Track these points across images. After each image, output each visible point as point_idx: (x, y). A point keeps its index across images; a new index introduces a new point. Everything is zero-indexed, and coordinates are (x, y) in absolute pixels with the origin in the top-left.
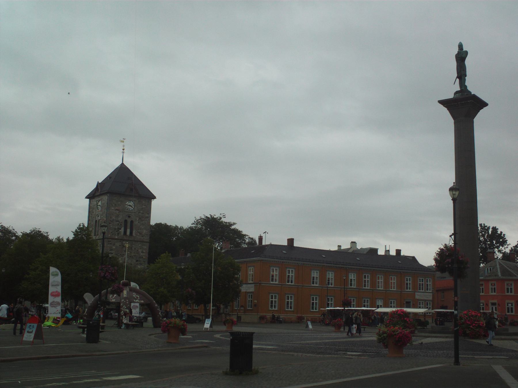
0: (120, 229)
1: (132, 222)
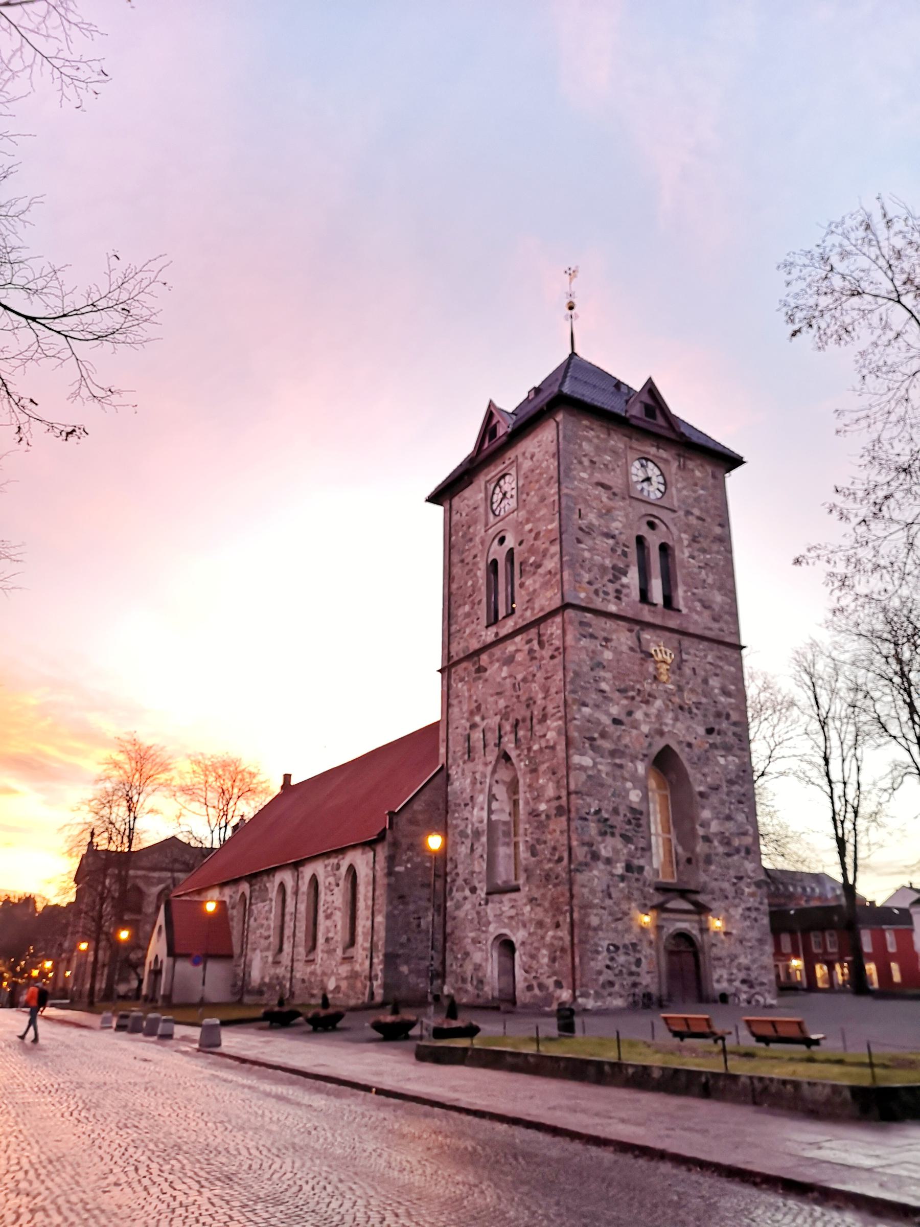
0: (625, 574)
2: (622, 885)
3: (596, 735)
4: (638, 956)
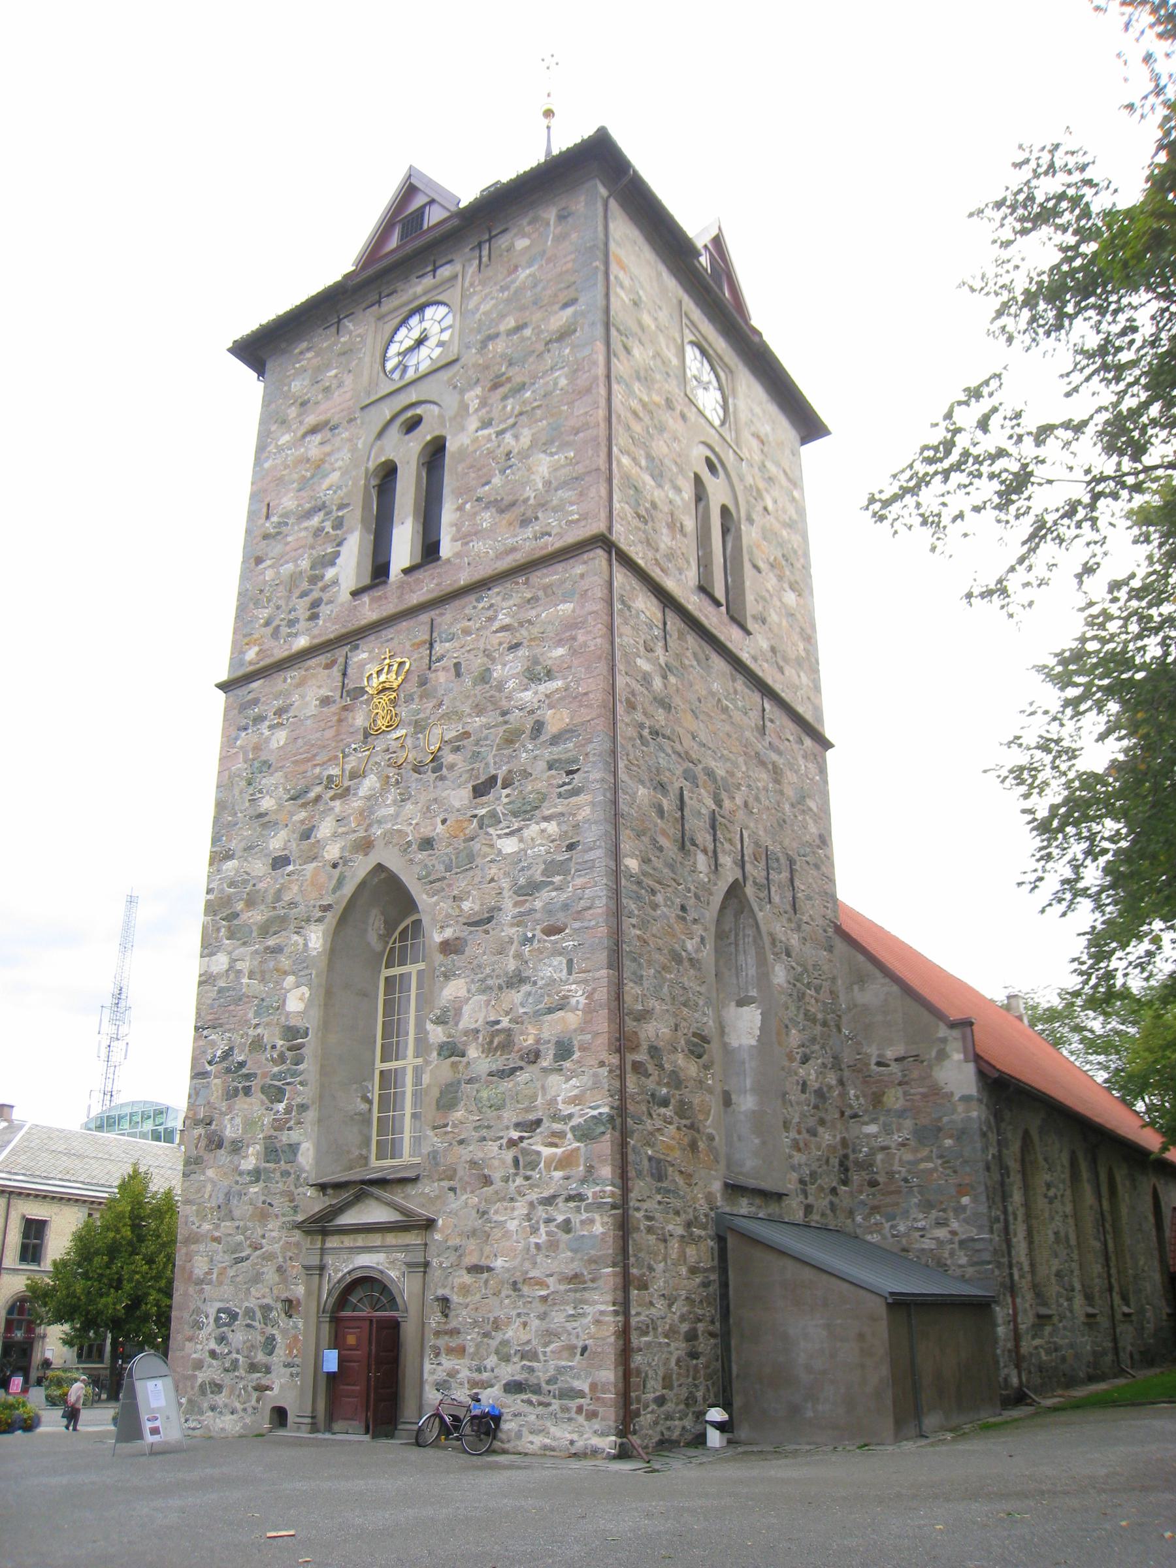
1: (436, 452)
2: (254, 1189)
3: (240, 906)
4: (270, 1330)
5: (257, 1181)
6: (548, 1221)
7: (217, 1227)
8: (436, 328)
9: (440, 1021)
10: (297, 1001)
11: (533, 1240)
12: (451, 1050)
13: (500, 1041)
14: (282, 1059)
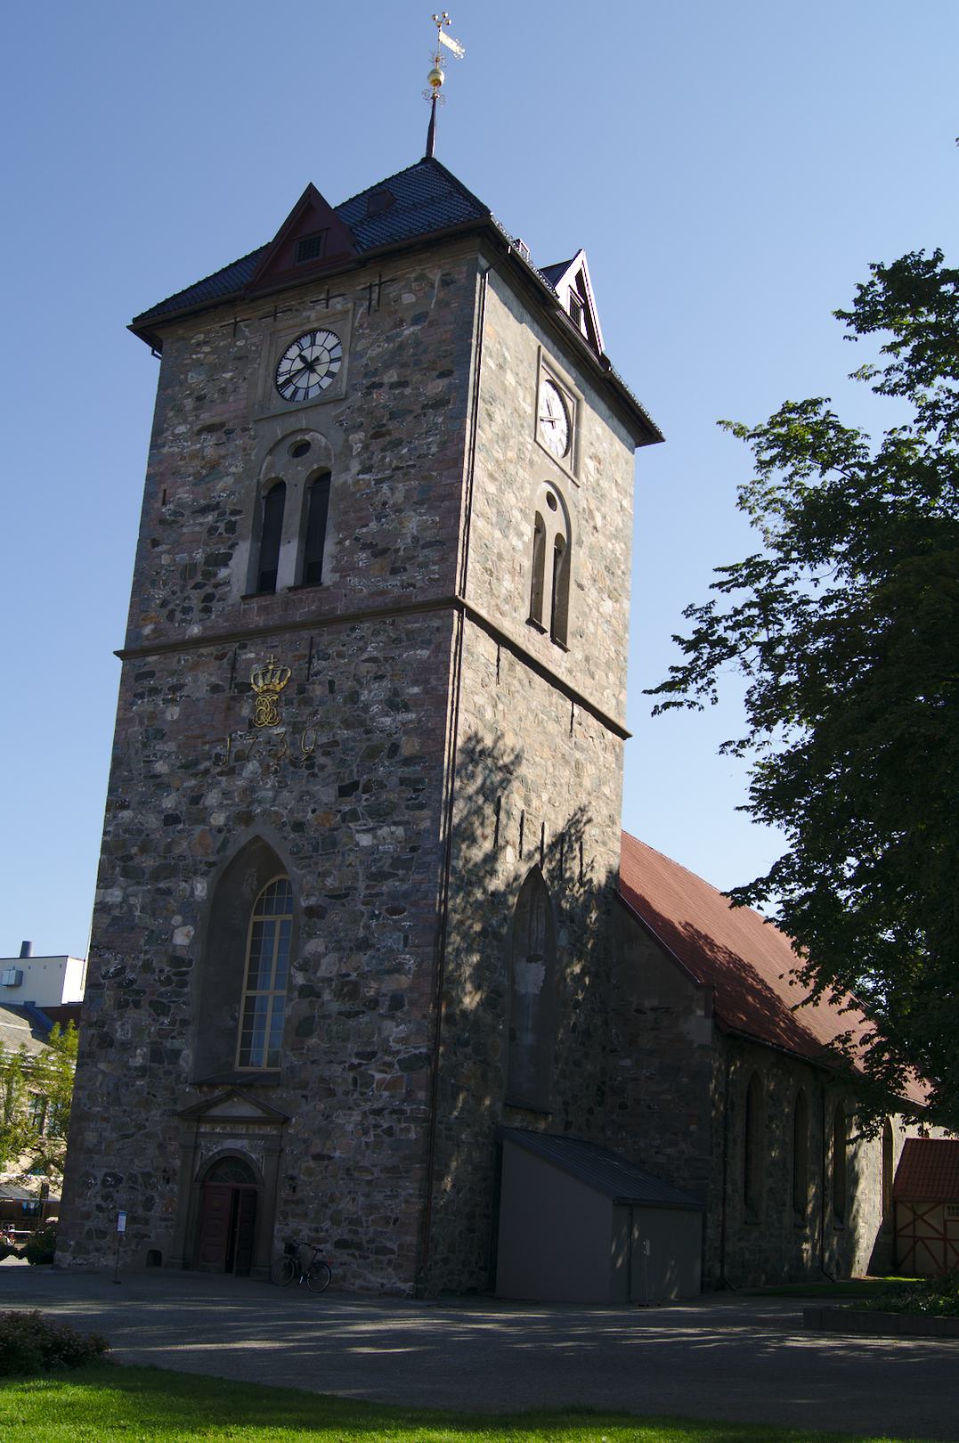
0: (224, 560)
1: (321, 480)
3: (134, 850)
5: (143, 1076)
6: (376, 1126)
7: (106, 1109)
8: (325, 357)
9: (300, 969)
10: (181, 938)
11: (364, 1139)
12: (309, 992)
13: (348, 989)
14: (168, 981)
